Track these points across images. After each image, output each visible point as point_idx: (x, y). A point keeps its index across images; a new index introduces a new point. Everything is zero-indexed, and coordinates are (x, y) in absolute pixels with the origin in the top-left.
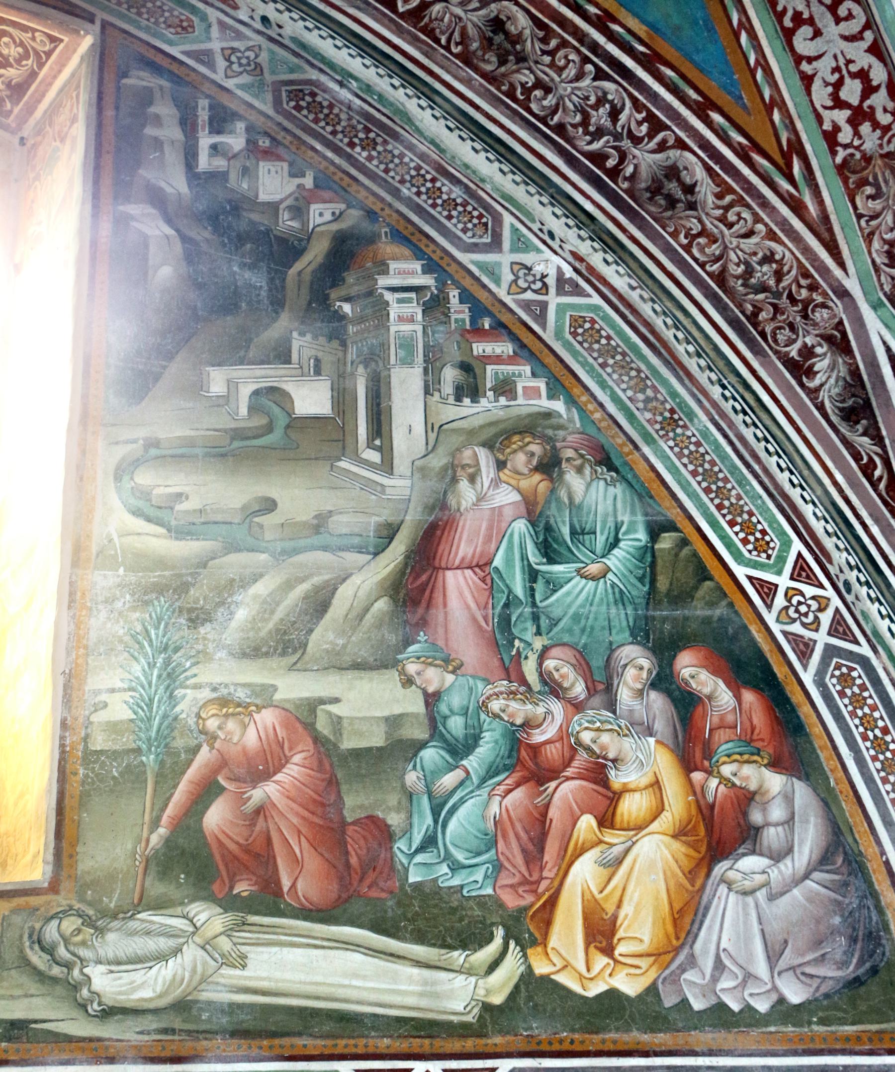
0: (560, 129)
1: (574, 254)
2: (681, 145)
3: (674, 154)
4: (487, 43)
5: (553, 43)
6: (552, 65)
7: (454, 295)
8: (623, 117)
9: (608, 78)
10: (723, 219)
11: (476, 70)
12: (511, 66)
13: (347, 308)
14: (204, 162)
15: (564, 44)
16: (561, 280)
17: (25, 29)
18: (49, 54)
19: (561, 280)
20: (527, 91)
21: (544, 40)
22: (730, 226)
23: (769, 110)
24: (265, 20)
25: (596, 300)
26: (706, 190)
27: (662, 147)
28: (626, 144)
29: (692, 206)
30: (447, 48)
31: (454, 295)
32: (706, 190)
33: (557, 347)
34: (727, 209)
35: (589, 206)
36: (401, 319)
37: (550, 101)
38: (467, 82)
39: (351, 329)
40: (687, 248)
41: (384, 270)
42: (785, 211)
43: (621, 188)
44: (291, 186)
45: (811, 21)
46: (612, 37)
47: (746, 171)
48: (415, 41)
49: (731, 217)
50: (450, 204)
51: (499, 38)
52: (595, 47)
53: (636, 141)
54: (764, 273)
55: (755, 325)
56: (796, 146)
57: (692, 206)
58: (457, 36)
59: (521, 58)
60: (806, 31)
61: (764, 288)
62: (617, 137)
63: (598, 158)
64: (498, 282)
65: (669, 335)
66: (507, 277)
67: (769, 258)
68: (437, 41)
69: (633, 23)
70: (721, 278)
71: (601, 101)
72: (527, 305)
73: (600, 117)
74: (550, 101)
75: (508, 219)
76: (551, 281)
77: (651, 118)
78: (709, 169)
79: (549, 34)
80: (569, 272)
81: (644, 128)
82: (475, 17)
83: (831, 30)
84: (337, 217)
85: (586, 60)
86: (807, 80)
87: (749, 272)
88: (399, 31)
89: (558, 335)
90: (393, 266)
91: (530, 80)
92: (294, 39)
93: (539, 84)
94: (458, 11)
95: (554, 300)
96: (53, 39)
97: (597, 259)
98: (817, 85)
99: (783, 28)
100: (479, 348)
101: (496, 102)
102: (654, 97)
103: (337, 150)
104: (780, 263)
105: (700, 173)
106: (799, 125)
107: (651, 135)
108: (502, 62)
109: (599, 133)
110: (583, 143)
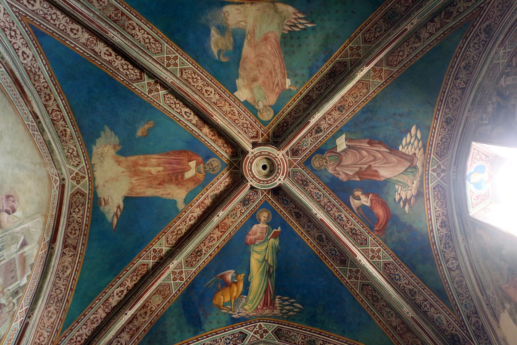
0: (480, 54)
1: (499, 47)
2: (480, 30)
3: (482, 31)
4: (468, 70)
5: (466, 57)
6: (469, 57)
7: (506, 71)
8: (476, 42)
9: (470, 46)
10: (492, 18)
11: (473, 71)
12: (471, 64)
13: (507, 93)
14: (487, 122)
15: (466, 55)
16: (504, 49)
17: (473, 154)
18: (478, 150)
19: (504, 49)
20: (474, 61)
21: (466, 59)
22: (493, 16)
23: (473, 13)
24: (469, 111)
25: (507, 41)
26: (487, 23)
27: (481, 33)
28: (481, 40)
29: (490, 25)
30: (470, 77)
31: (506, 71)
32: (487, 23)
33: (514, 48)
34: (490, 18)
35: (491, 46)
36: (509, 81)
37: (475, 56)
38: (475, 72)
39: (511, 92)
40: (497, 24)
41: (502, 85)
42: (489, 6)
43: (488, 40)
44: (490, 105)
45: (458, 9)
46: (463, 46)
47: (484, 15)
48: (470, 83)
49: (491, 16)
50: (493, 74)
51: (467, 67)
52: (465, 49)
53: (480, 38)
54: (500, 7)
55: (509, 6)
56: (479, 6)
57: (490, 25)
58: (468, 75)
59: (469, 63)
60: (459, 10)
61: (503, 6)
62: (480, 42)
63: (483, 45)
64: (504, 62)
65: (510, 24)
66: (504, 60)
67: (498, 7)
68: (469, 79)
69: (461, 42)
70: (501, 16)
71: (474, 46)
72: (508, 55)
73: (476, 46)
74: (475, 56)
75: (495, 62)
76: (504, 51)
77: (476, 36)
78: (484, 23)
79: (464, 58)
80: (503, 48)
81: (478, 37)
82: (464, 72)
83: (459, 5)
84: (495, 96)
85: (468, 51)
86: (468, 7)
87: (500, 10)
88: (469, 86)
89: (512, 48)
90: (502, 84)
91: (473, 61)
92: (471, 105)
93: (473, 59)
94: (464, 75)
95: (508, 50)
96: (474, 149)
97: (499, 42)
98: (468, 5)
99: (460, 14)
100: (514, 65)
101: (477, 66)
102: (472, 36)
103: (486, 96)
104: (498, 4)
105: (485, 25)
106: (475, 7)
107: (479, 36)
108: (470, 66)
109: (479, 46)
110: (481, 49)
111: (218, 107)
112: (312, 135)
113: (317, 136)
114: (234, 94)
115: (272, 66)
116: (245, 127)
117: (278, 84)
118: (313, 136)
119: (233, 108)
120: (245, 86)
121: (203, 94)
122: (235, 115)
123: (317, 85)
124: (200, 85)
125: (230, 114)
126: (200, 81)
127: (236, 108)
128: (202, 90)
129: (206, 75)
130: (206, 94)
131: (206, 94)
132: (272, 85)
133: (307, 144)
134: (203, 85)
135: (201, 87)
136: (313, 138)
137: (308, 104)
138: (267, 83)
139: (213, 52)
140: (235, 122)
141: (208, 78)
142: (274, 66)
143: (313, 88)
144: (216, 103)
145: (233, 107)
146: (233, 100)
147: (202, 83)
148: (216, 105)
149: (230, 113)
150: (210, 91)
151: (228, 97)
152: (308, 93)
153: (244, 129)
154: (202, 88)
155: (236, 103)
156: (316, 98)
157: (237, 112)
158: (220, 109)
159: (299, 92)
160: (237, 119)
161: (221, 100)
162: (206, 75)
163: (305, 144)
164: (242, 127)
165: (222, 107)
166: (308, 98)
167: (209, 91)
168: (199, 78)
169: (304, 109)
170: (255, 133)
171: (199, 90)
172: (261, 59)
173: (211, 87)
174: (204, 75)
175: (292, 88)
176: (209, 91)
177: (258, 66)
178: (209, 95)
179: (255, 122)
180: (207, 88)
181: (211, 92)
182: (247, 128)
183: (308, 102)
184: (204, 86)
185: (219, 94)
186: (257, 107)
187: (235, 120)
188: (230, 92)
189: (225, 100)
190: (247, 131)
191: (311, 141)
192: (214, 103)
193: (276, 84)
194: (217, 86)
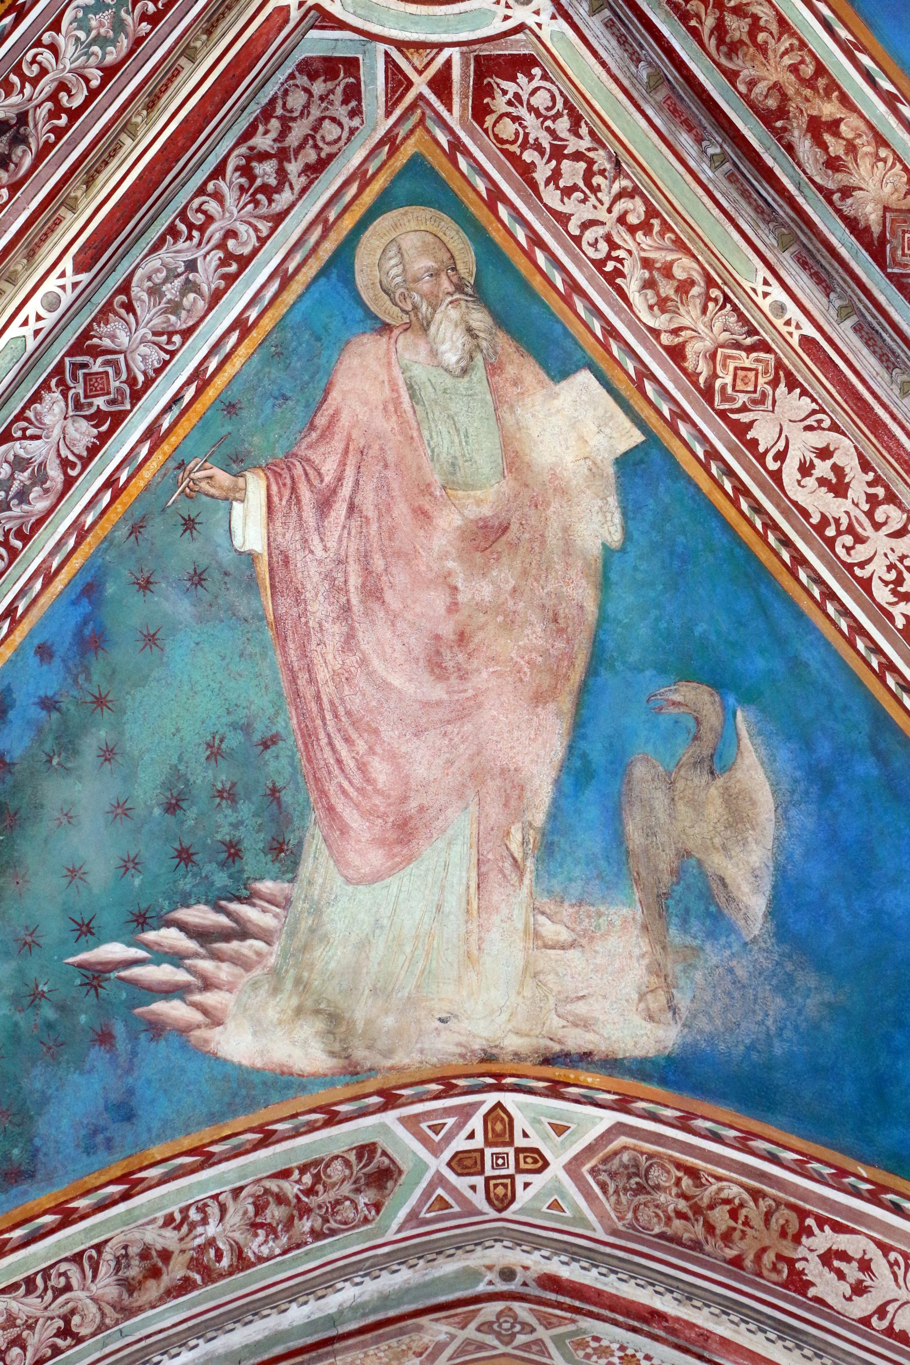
111: (768, 350)
112: (53, 97)
113: (14, 99)
114: (638, 437)
115: (366, 641)
116: (577, 156)
117: (324, 505)
118: (47, 85)
119: (659, 321)
120: (563, 491)
121: (866, 466)
122: (647, 263)
123: (41, 506)
124: (879, 541)
125: (679, 273)
126: (878, 568)
127: (630, 326)
128: (873, 500)
129: (830, 609)
130: (847, 459)
131: (847, 459)
132: (368, 501)
133: (82, 24)
134: (860, 540)
135: (877, 526)
136: (44, 72)
137: (96, 352)
138: (401, 510)
139: (769, 763)
140: (652, 212)
141: (818, 580)
142: (349, 640)
143: (69, 482)
144: (775, 383)
145: (656, 333)
146: (649, 387)
147: (861, 553)
148: (779, 365)
149: (684, 287)
150: (810, 482)
151: (686, 418)
152: (104, 438)
153: (585, 144)
154: (870, 514)
155: (630, 366)
156: (36, 398)
157: (632, 287)
158: (753, 332)
159: (166, 448)
160: (633, 230)
161: (742, 398)
162: (830, 609)
163: (106, 17)
164: (601, 159)
165: (737, 346)
166: (100, 402)
167: (822, 482)
168: (882, 594)
169: (129, 307)
170: (500, 104)
171: (892, 498)
172: (438, 692)
173: (806, 514)
174: (845, 612)
175: (223, 478)
176: (822, 482)
177: (462, 638)
178: (825, 453)
179: (496, 196)
180: (836, 507)
181: (805, 469)
182: (558, 153)
183: (97, 366)
184: (851, 530)
185: (753, 444)
186: (480, 319)
187: (645, 227)
188: (668, 455)
189: (708, 393)
190: (563, 125)
191: (53, 48)
192: (792, 384)
193: (340, 509)
194: (758, 509)
